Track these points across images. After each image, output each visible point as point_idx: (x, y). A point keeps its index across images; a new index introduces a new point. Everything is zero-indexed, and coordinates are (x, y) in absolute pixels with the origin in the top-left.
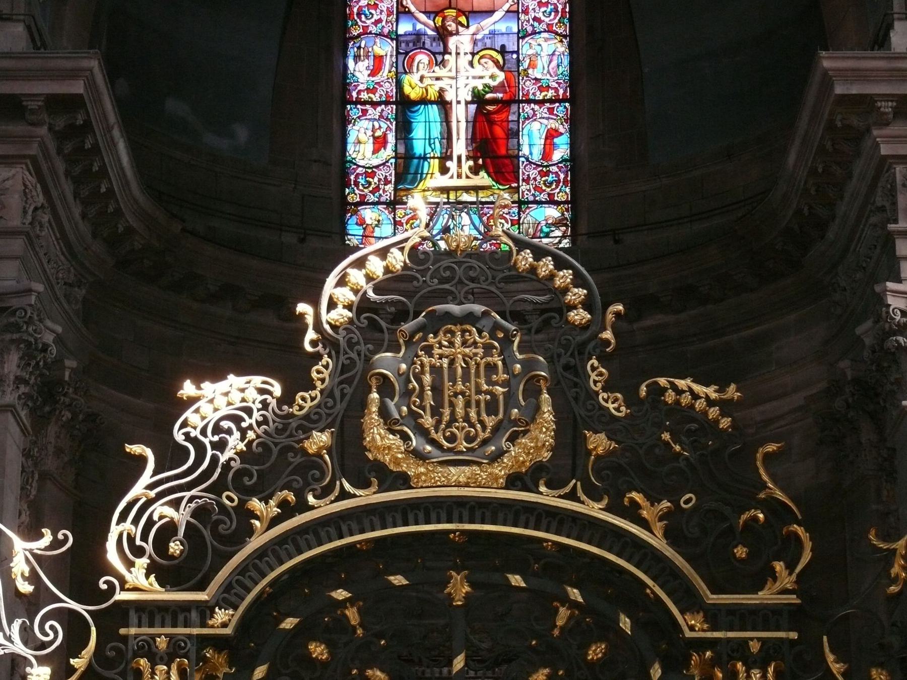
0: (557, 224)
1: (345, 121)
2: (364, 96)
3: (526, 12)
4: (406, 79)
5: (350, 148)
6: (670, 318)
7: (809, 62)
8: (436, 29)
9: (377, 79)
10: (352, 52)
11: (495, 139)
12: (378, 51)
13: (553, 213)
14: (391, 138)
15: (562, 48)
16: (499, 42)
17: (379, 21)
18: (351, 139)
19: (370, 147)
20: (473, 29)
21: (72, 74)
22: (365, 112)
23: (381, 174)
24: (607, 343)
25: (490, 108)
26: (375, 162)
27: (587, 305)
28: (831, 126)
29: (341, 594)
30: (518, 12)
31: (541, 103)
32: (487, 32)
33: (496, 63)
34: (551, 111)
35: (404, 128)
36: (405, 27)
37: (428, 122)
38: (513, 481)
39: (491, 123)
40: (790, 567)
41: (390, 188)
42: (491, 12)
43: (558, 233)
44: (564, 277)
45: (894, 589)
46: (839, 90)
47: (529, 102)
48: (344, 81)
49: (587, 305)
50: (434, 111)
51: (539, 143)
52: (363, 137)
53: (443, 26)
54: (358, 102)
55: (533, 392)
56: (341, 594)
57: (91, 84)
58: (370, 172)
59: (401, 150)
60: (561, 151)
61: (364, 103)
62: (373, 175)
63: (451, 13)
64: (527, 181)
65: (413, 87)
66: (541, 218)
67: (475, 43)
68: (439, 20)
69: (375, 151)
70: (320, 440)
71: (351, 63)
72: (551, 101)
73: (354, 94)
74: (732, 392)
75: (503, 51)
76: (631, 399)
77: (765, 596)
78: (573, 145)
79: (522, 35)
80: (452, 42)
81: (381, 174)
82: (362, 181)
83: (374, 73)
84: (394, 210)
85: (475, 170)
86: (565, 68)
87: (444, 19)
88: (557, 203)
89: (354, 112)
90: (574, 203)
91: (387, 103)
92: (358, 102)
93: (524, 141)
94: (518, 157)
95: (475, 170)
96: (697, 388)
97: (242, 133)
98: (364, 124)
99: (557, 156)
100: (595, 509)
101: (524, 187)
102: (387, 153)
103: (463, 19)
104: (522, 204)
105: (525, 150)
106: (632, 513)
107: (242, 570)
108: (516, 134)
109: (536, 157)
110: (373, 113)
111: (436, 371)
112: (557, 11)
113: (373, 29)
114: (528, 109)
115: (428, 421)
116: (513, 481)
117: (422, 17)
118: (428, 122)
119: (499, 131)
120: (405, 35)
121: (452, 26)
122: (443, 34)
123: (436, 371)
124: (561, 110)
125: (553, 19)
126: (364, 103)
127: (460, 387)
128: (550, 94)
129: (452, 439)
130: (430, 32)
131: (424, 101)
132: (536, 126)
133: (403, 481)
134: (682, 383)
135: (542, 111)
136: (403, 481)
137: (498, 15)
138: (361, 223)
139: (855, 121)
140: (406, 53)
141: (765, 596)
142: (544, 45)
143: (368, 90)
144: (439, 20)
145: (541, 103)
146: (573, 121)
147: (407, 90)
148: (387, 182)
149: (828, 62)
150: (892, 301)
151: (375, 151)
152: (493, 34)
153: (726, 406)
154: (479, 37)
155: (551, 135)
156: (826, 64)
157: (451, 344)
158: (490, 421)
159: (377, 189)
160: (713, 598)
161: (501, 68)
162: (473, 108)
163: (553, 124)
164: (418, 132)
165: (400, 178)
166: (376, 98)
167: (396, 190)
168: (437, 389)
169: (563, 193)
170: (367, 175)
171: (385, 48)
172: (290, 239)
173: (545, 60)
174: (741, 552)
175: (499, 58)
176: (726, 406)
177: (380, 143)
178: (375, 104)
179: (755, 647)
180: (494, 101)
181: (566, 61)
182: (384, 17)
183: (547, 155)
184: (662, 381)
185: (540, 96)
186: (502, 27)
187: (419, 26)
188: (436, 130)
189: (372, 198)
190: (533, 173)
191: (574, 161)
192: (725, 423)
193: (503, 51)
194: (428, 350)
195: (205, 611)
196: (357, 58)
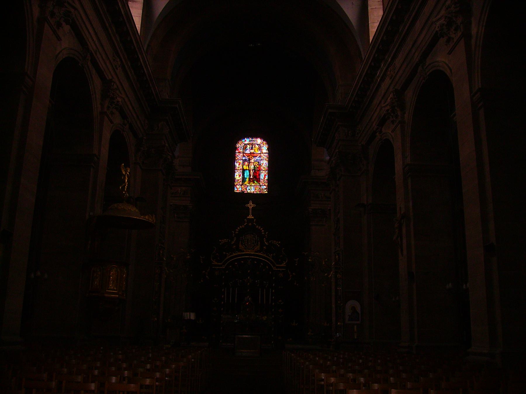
0: (266, 189)
1: (235, 172)
2: (238, 169)
3: (262, 156)
4: (244, 166)
5: (235, 176)
8: (248, 159)
9: (239, 166)
10: (236, 162)
11: (257, 176)
12: (240, 161)
13: (265, 187)
14: (241, 175)
17: (240, 157)
18: (235, 175)
19: (238, 176)
20: (254, 159)
22: (238, 171)
24: (266, 236)
25: (256, 171)
26: (239, 179)
27: (264, 232)
30: (260, 157)
31: (264, 170)
32: (256, 159)
33: (257, 164)
34: (265, 172)
36: (244, 158)
37: (247, 173)
39: (256, 173)
40: (285, 262)
41: (241, 182)
42: (257, 156)
43: (265, 190)
45: (296, 265)
47: (262, 170)
48: (235, 166)
49: (264, 232)
50: (248, 171)
51: (263, 177)
52: (237, 175)
53: (250, 158)
54: (237, 169)
58: (238, 180)
59: (243, 177)
61: (238, 170)
62: (239, 181)
63: (251, 156)
64: (261, 182)
65: (245, 167)
66: (263, 188)
67: (254, 161)
68: (249, 157)
69: (239, 177)
71: (236, 163)
72: (265, 170)
73: (236, 168)
75: (258, 162)
79: (261, 160)
80: (251, 160)
81: (240, 180)
82: (237, 181)
83: (239, 165)
84: (242, 186)
85: (252, 216)
86: (267, 165)
87: (250, 157)
88: (266, 186)
89: (236, 171)
90: (268, 186)
91: (241, 170)
92: (237, 169)
94: (260, 179)
95: (252, 216)
96: (276, 242)
98: (237, 173)
99: (266, 178)
101: (261, 183)
102: (241, 177)
103: (253, 157)
104: (260, 186)
105: (261, 177)
108: (260, 175)
109: (263, 178)
110: (239, 171)
112: (266, 156)
113: (239, 158)
114: (261, 171)
115: (246, 245)
117: (247, 157)
118: (247, 173)
119: (257, 175)
120: (244, 159)
122: (249, 159)
124: (267, 172)
125: (266, 158)
126: (238, 170)
127: (250, 241)
128: (265, 169)
129: (249, 247)
130: (248, 159)
131: (247, 170)
132: (263, 174)
134: (274, 241)
135: (264, 172)
138: (237, 188)
140: (244, 162)
142: (265, 162)
143: (238, 168)
144: (249, 157)
145: (264, 170)
146: (268, 173)
147: (244, 168)
148: (241, 182)
151: (239, 177)
152: (257, 159)
154: (255, 160)
155: (265, 175)
157: (249, 236)
158: (253, 245)
159: (239, 183)
160: (277, 265)
161: (258, 165)
162: (254, 171)
164: (245, 174)
166: (239, 169)
167: (242, 183)
170: (238, 180)
171: (241, 162)
173: (265, 164)
174: (280, 260)
175: (258, 163)
177: (240, 176)
178: (239, 170)
179: (281, 271)
180: (257, 170)
181: (268, 164)
182: (241, 157)
183: (264, 178)
184: (272, 241)
185: (263, 170)
186: (258, 159)
187: (246, 158)
188: (248, 174)
189: (238, 184)
190: (262, 181)
191: (268, 180)
194: (247, 237)
196: (237, 163)
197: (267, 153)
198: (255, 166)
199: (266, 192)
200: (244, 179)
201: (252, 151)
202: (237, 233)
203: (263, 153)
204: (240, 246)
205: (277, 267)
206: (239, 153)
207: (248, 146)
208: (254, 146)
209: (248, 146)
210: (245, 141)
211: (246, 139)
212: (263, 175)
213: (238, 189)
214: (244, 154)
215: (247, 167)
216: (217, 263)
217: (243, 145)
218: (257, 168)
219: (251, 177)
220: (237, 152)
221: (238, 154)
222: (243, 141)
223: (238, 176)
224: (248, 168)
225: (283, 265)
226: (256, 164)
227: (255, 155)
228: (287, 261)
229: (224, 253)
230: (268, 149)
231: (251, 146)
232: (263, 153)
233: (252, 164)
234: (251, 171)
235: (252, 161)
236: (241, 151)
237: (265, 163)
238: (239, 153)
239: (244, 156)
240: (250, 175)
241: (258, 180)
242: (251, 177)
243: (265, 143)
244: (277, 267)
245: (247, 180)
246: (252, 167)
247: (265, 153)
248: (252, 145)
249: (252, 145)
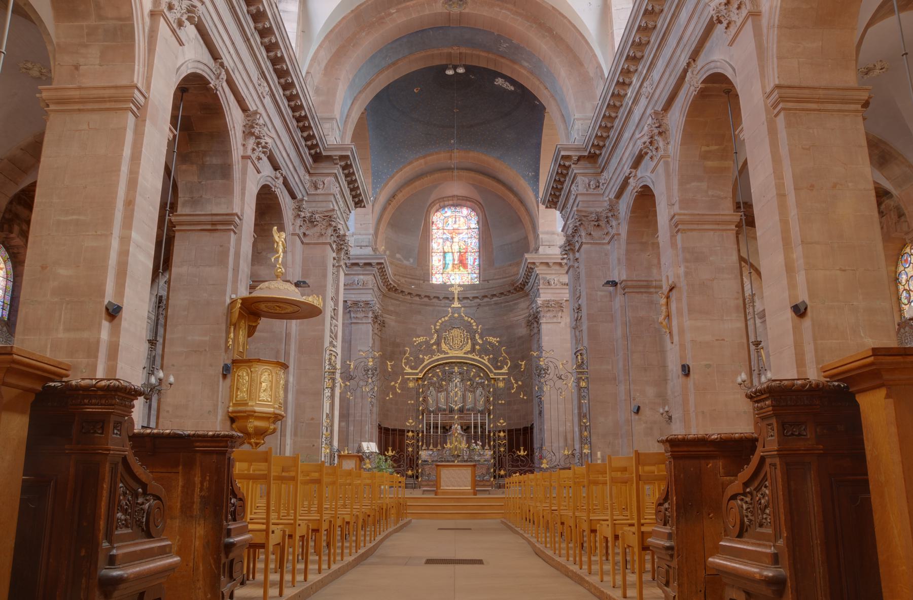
4: (445, 247)
6: (499, 299)
7: (523, 256)
10: (433, 242)
13: (475, 275)
14: (442, 259)
15: (477, 241)
16: (464, 239)
21: (382, 258)
23: (440, 267)
28: (527, 267)
29: (438, 371)
35: (444, 257)
36: (445, 236)
38: (465, 353)
44: (472, 321)
46: (528, 261)
51: (472, 261)
55: (467, 339)
56: (438, 371)
57: (385, 260)
60: (477, 263)
63: (454, 233)
70: (435, 347)
71: (433, 244)
74: (498, 339)
75: (465, 241)
76: (482, 340)
77: (503, 371)
78: (479, 261)
81: (440, 267)
86: (478, 245)
90: (479, 273)
93: (469, 260)
97: (411, 260)
99: (476, 263)
100: (477, 358)
102: (441, 263)
105: (469, 263)
106: (483, 358)
107: (423, 367)
109: (472, 264)
110: (438, 254)
111: (453, 336)
116: (465, 353)
119: (464, 258)
121: (454, 236)
122: (452, 238)
123: (453, 336)
124: (477, 254)
125: (475, 235)
133: (448, 353)
136: (448, 353)
137: (464, 233)
139: (532, 267)
141: (503, 371)
149: (526, 256)
150: (538, 302)
153: (497, 342)
155: (475, 259)
156: (526, 256)
163: (475, 257)
164: (447, 259)
165: (444, 268)
168: (453, 339)
169: (477, 271)
171: (441, 241)
172: (422, 282)
176: (497, 342)
177: (440, 261)
183: (474, 264)
186: (465, 236)
188: (451, 258)
192: (497, 344)
193: (465, 241)
195: (417, 374)
197: (476, 228)
198: (460, 249)
199: (478, 282)
200: (445, 266)
201: (456, 226)
202: (438, 327)
203: (471, 229)
204: (443, 345)
205: (495, 374)
206: (438, 229)
207: (450, 220)
208: (457, 219)
209: (450, 220)
210: (446, 212)
211: (446, 210)
212: (472, 259)
213: (437, 279)
214: (445, 231)
215: (450, 248)
216: (410, 371)
217: (442, 218)
218: (464, 249)
219: (456, 262)
220: (434, 227)
221: (436, 231)
222: (443, 212)
223: (436, 261)
224: (450, 251)
225: (505, 370)
226: (462, 244)
227: (460, 231)
228: (509, 365)
229: (421, 356)
230: (478, 222)
231: (454, 219)
232: (471, 229)
233: (457, 244)
234: (455, 254)
235: (456, 240)
236: (440, 225)
237: (474, 243)
238: (438, 229)
239: (444, 233)
240: (454, 260)
241: (465, 266)
242: (456, 262)
243: (473, 214)
244: (495, 374)
245: (450, 266)
246: (456, 248)
247: (473, 229)
248: (456, 218)
249: (456, 218)
